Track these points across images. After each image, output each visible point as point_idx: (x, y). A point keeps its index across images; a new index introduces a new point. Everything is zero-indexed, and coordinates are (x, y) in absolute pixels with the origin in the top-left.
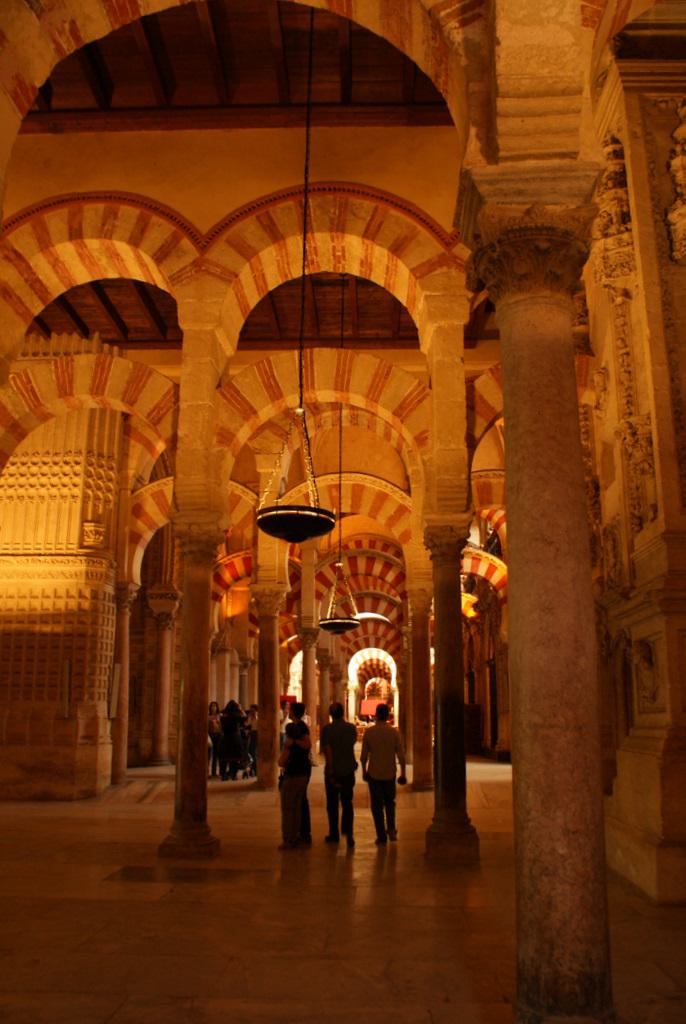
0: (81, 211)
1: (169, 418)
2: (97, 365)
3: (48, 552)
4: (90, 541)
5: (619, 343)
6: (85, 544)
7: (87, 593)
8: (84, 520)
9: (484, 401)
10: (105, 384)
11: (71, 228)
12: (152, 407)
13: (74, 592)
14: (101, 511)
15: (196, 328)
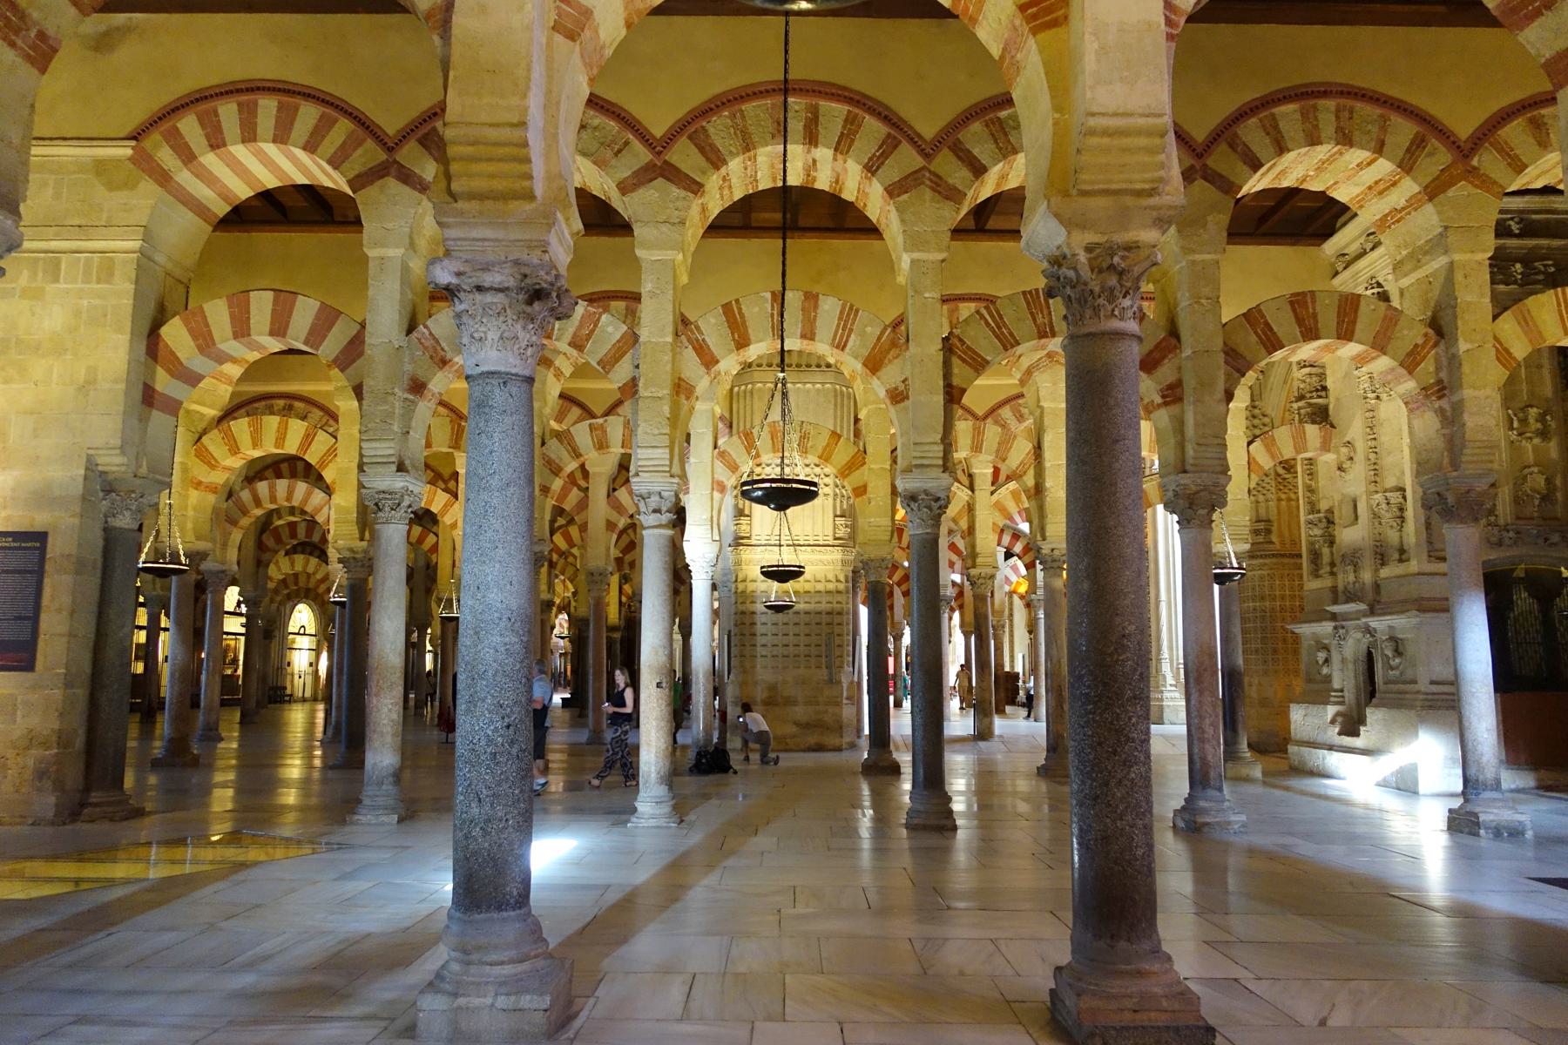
0: (957, 309)
1: (1031, 472)
2: (974, 429)
3: (807, 543)
4: (840, 534)
5: (1368, 430)
6: (837, 535)
7: (842, 579)
8: (836, 516)
9: (1257, 463)
10: (982, 444)
11: (951, 322)
12: (1018, 462)
13: (831, 577)
14: (845, 507)
15: (1052, 405)
